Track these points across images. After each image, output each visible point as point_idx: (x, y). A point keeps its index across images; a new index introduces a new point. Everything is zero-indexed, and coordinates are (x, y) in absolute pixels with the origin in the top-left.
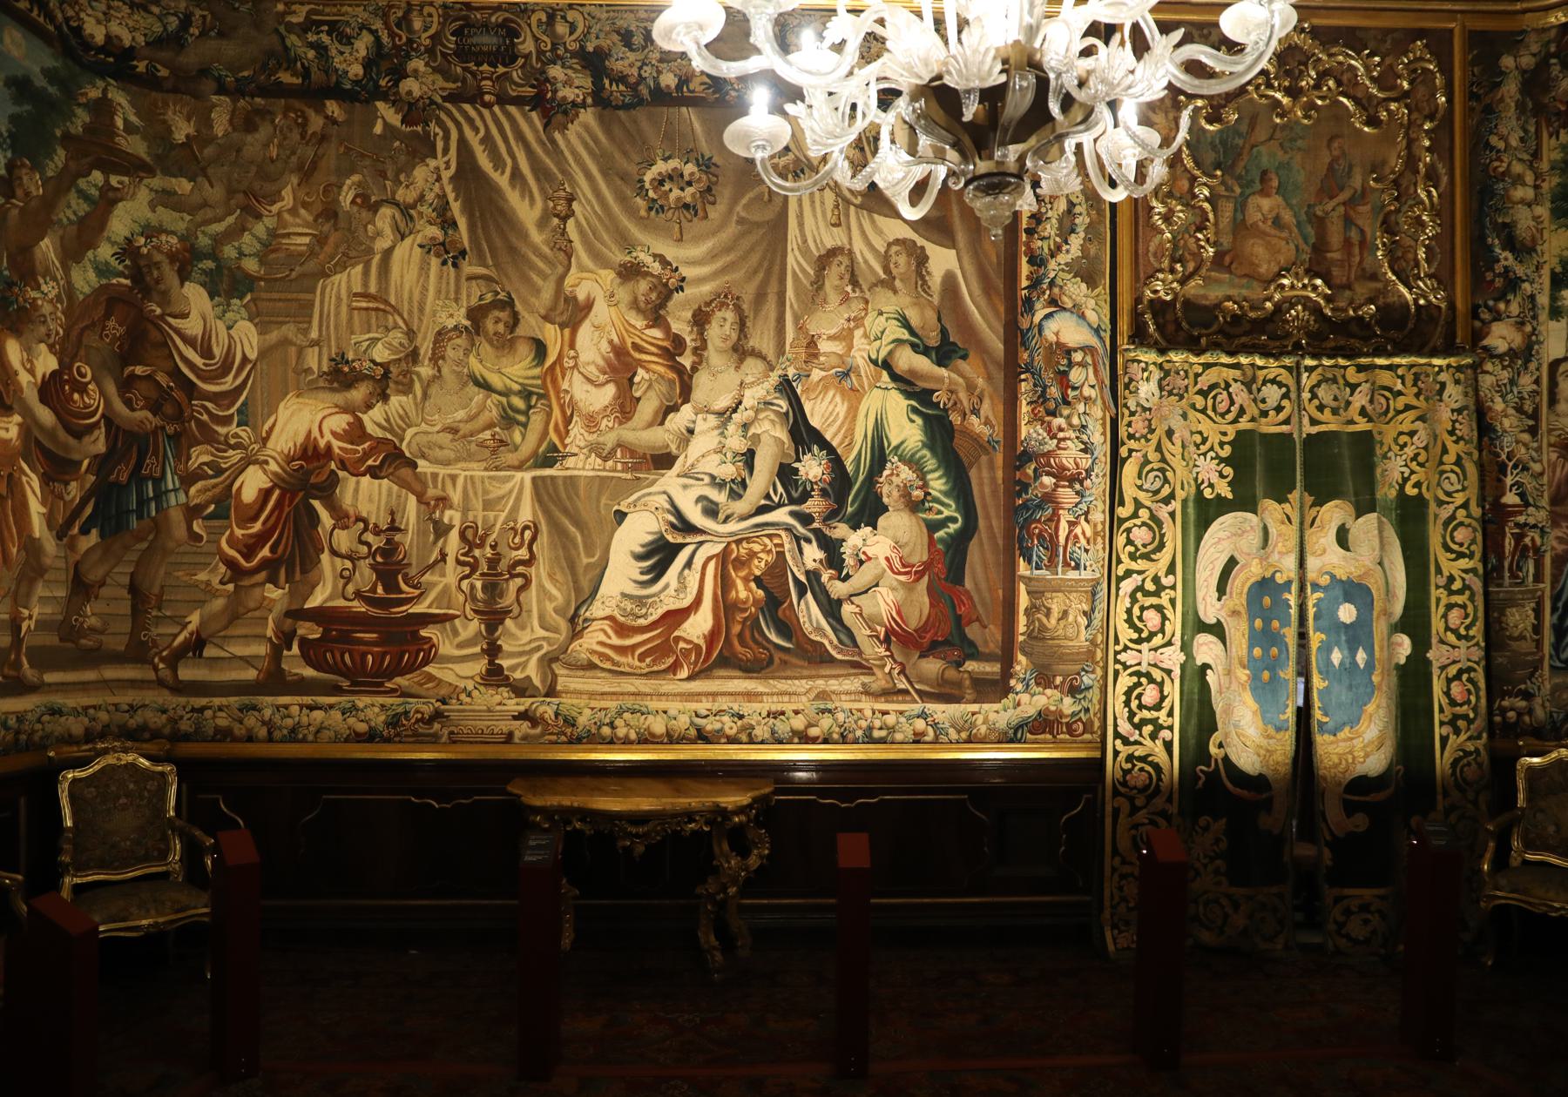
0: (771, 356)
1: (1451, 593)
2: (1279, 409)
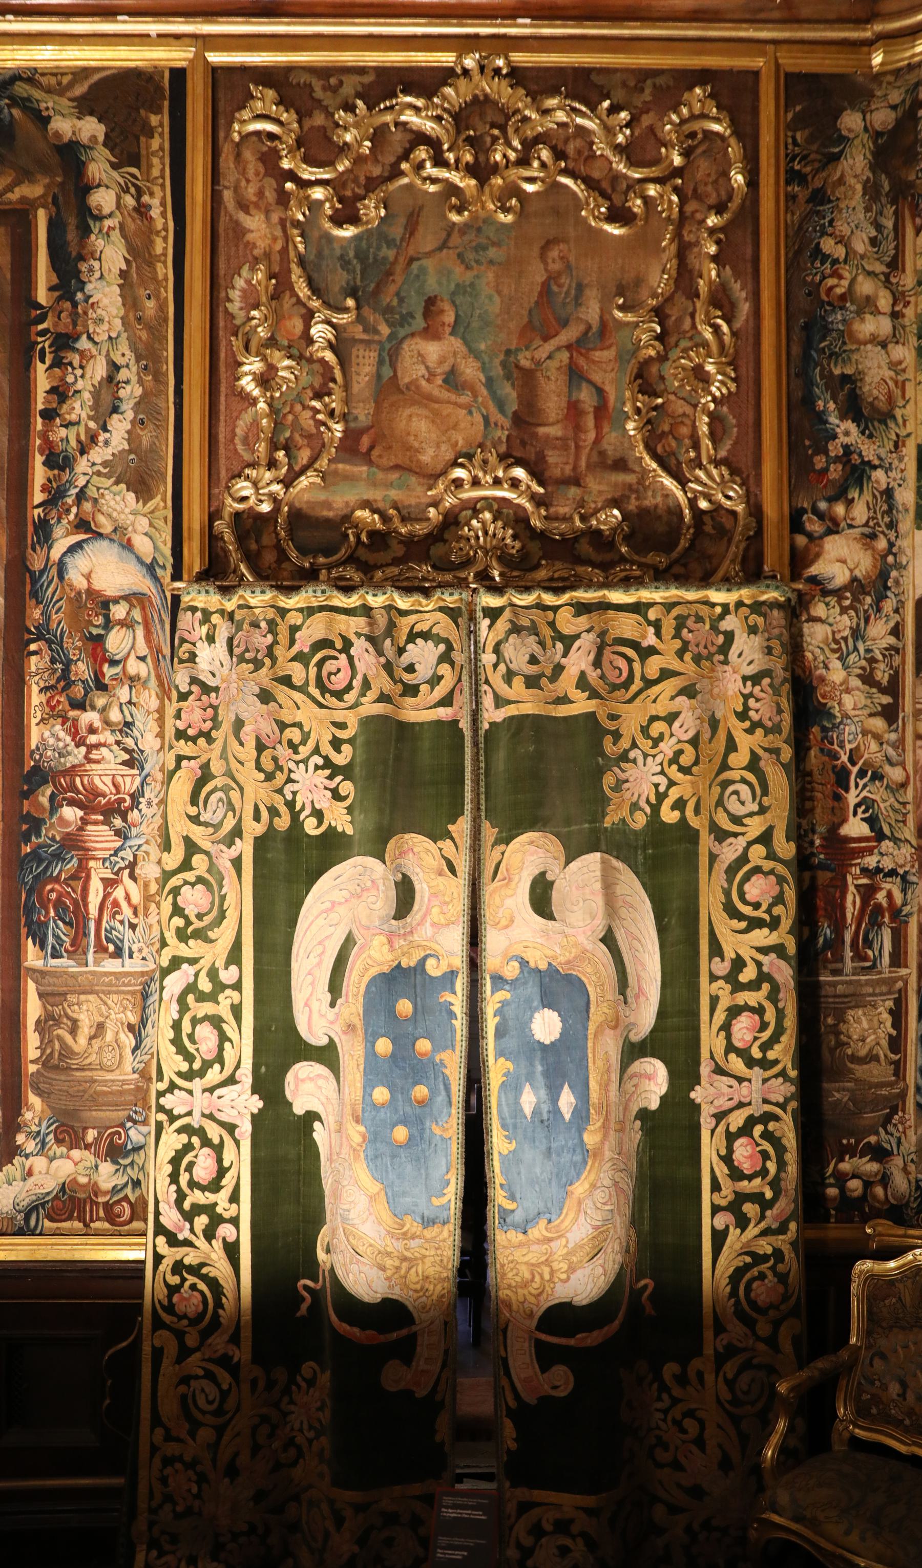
1: (738, 987)
2: (436, 680)
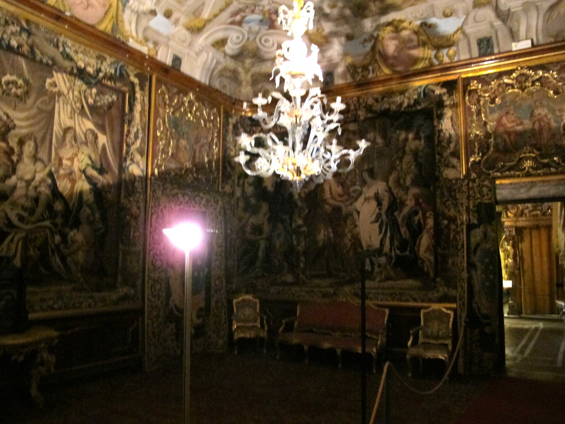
0: (46, 162)
